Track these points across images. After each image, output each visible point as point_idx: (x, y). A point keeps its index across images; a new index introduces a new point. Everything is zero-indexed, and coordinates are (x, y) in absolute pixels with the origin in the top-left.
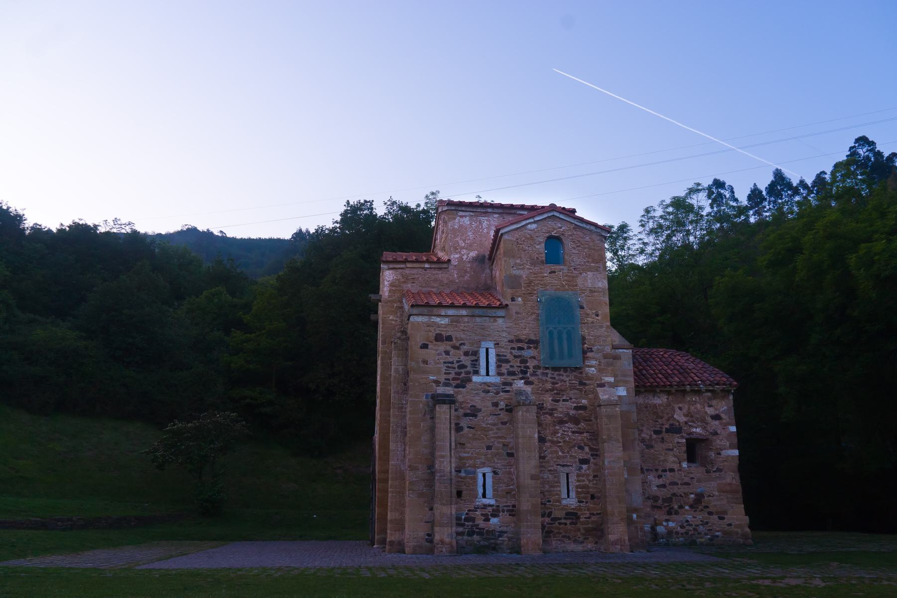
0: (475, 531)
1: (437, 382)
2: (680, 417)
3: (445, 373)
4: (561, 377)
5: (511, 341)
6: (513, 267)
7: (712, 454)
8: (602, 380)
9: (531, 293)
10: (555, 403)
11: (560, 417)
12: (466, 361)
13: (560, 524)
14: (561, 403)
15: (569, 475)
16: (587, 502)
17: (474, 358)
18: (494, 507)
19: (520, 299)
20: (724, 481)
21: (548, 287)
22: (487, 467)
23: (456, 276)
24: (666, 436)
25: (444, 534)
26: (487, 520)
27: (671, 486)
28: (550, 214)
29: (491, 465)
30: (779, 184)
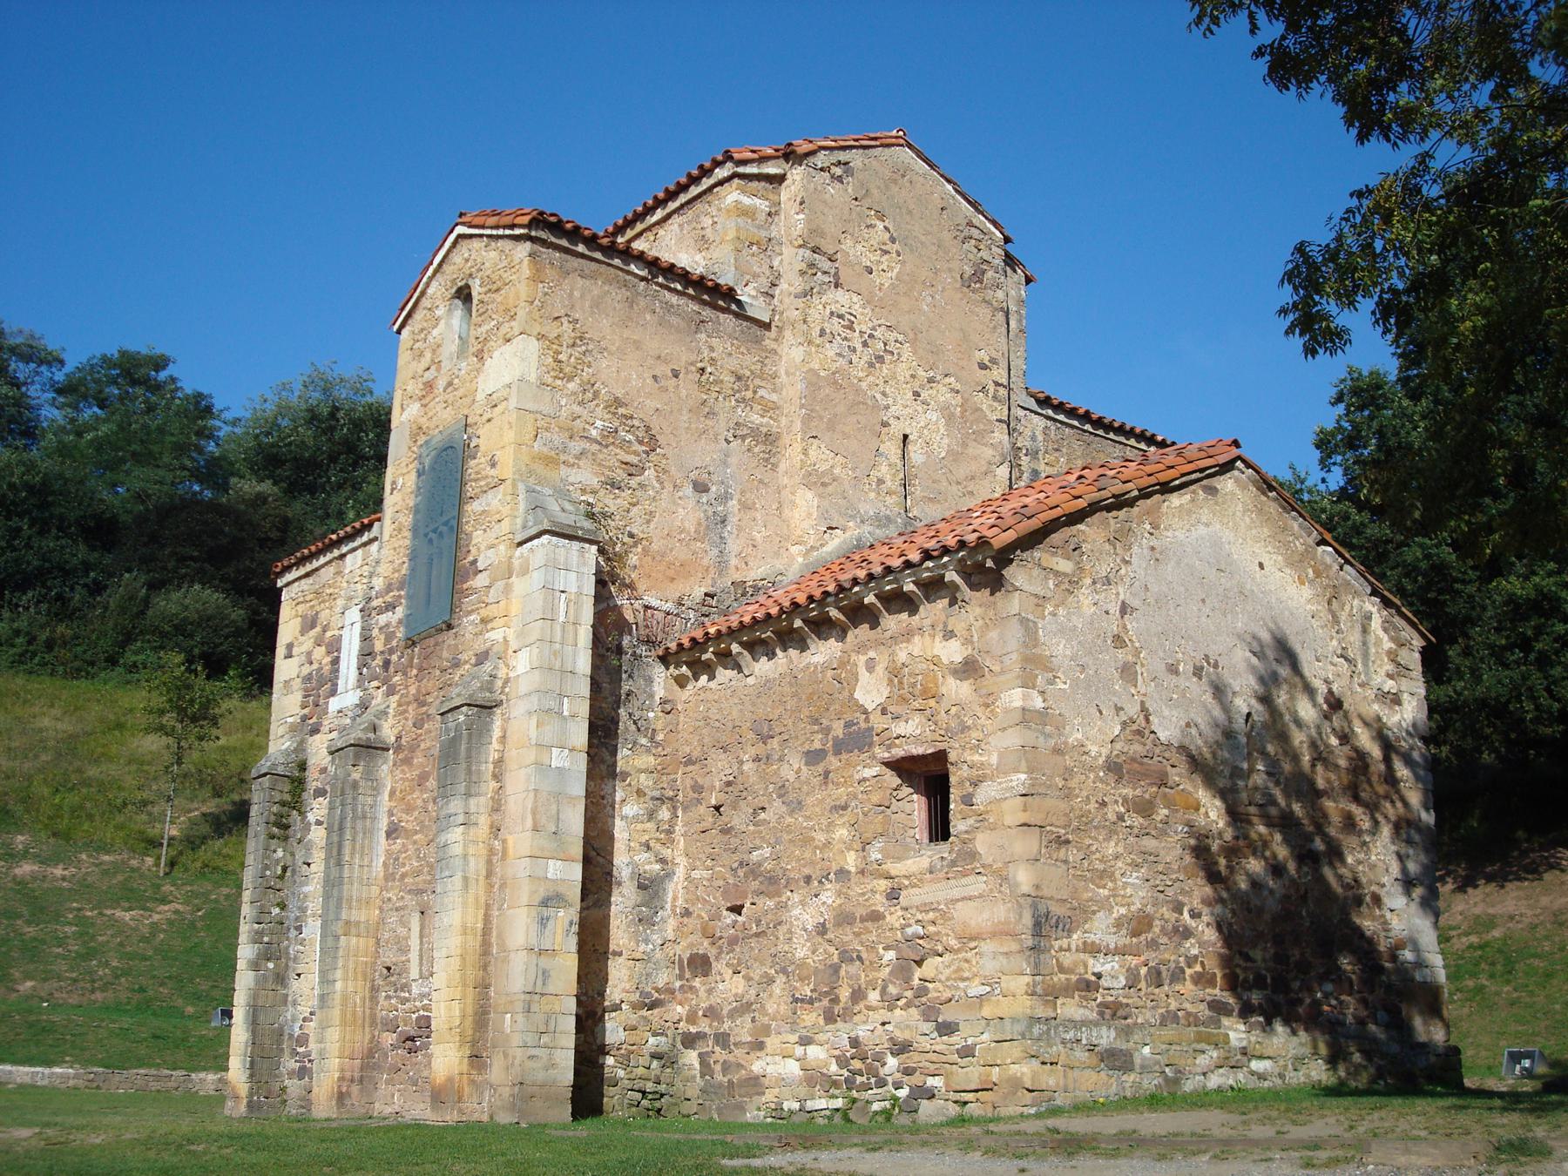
24: (833, 762)
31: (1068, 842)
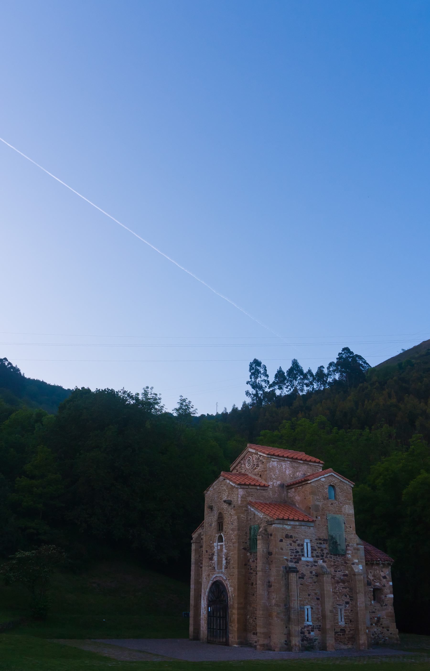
0: (304, 639)
1: (287, 560)
3: (291, 555)
4: (337, 559)
5: (316, 539)
6: (316, 500)
7: (383, 597)
8: (353, 561)
9: (324, 515)
10: (335, 573)
11: (337, 580)
12: (299, 549)
13: (338, 635)
14: (338, 572)
15: (342, 610)
16: (348, 624)
17: (302, 548)
18: (312, 627)
19: (319, 517)
20: (388, 611)
21: (331, 512)
22: (309, 605)
23: (271, 494)
25: (296, 641)
26: (309, 633)
28: (331, 474)
29: (310, 604)
30: (295, 370)
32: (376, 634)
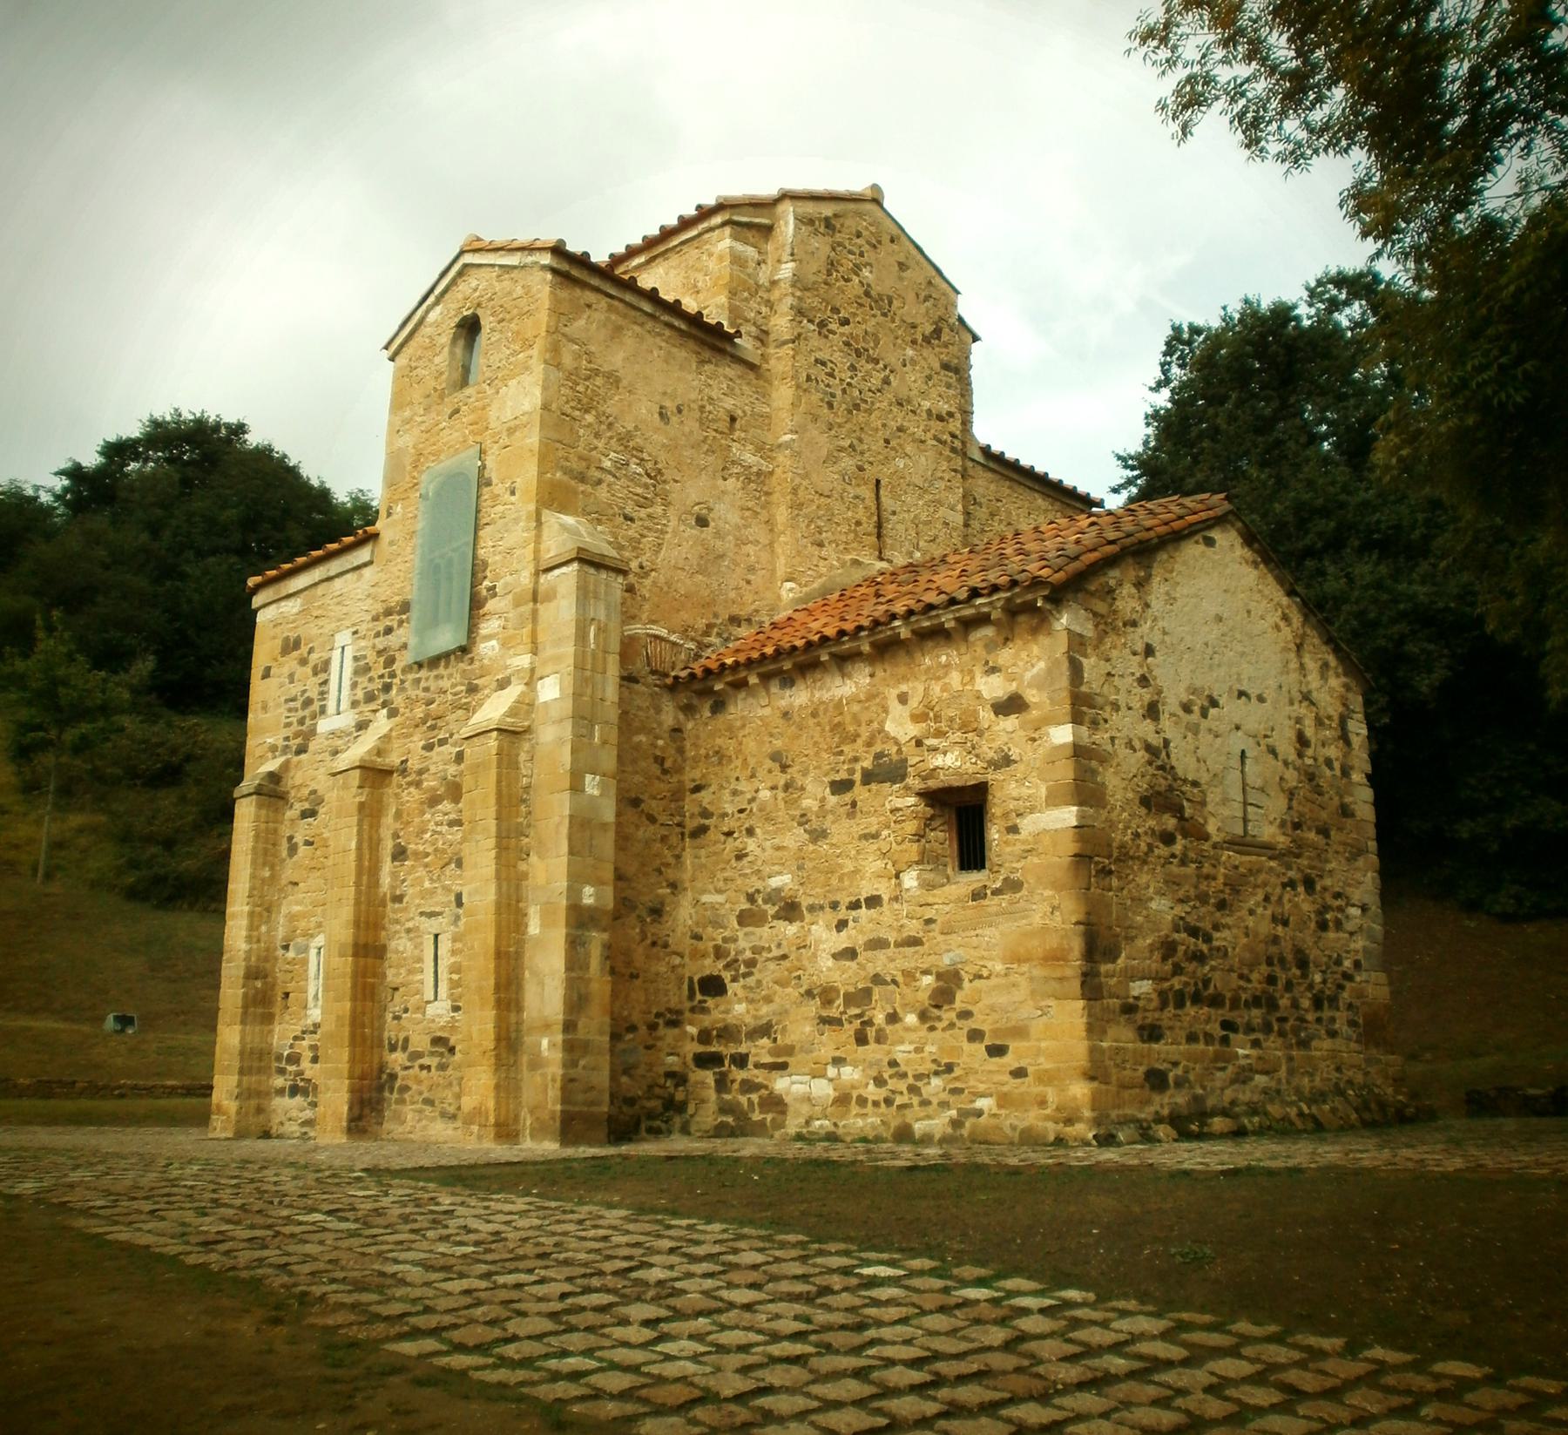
2: (900, 726)
5: (376, 619)
13: (422, 1067)
14: (437, 749)
24: (860, 792)
27: (870, 954)
31: (1110, 872)
32: (904, 1075)
